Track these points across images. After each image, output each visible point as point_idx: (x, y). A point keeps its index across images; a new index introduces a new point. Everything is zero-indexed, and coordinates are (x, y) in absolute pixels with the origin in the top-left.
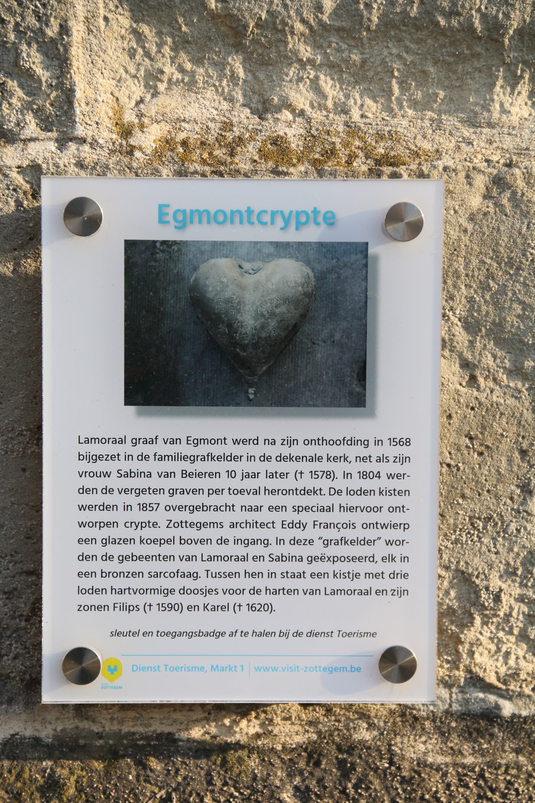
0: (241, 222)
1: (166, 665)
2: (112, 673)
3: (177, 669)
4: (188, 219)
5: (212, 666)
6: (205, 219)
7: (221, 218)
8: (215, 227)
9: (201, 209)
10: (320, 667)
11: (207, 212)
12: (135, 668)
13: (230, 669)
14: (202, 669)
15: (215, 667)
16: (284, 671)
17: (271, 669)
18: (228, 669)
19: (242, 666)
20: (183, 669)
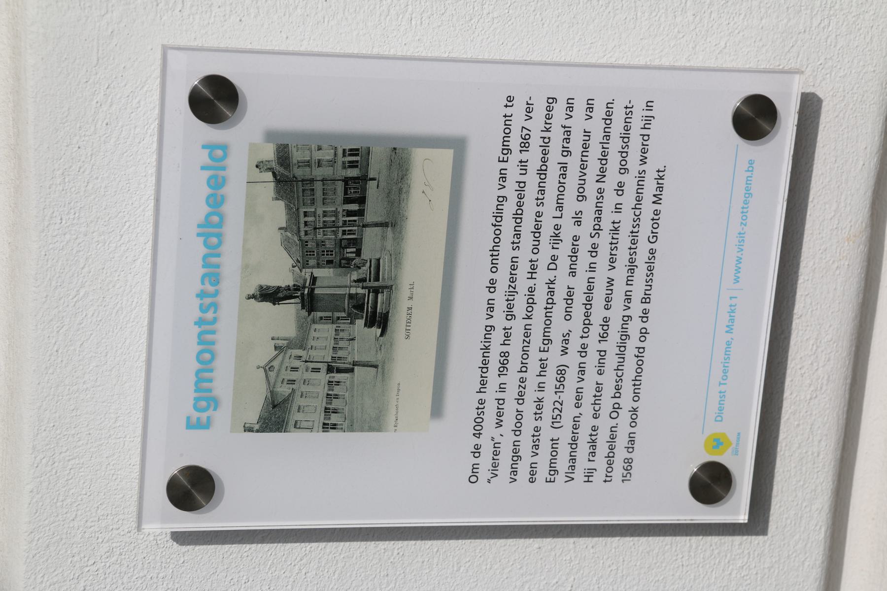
0: (214, 332)
1: (720, 384)
2: (722, 444)
3: (725, 372)
4: (206, 394)
5: (727, 332)
6: (207, 375)
7: (207, 356)
8: (218, 363)
9: (193, 379)
11: (198, 373)
13: (733, 311)
14: (729, 344)
15: (728, 329)
16: (742, 250)
17: (738, 265)
19: (731, 298)
20: (726, 365)
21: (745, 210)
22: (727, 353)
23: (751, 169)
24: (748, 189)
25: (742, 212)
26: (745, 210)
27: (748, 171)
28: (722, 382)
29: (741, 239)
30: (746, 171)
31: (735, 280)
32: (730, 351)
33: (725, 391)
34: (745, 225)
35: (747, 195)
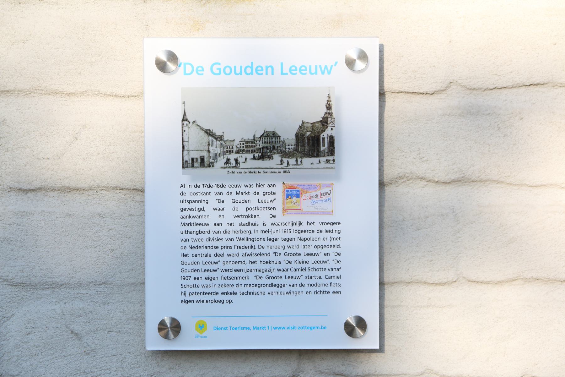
3: (236, 329)
5: (254, 327)
10: (306, 327)
12: (215, 328)
13: (263, 328)
14: (248, 328)
16: (288, 329)
18: (261, 328)
19: (268, 327)
21: (305, 328)
22: (244, 328)
23: (322, 328)
24: (314, 328)
25: (304, 327)
26: (305, 328)
27: (322, 327)
28: (232, 328)
29: (293, 328)
30: (321, 326)
31: (275, 327)
32: (245, 329)
33: (227, 330)
34: (299, 329)
35: (311, 328)
